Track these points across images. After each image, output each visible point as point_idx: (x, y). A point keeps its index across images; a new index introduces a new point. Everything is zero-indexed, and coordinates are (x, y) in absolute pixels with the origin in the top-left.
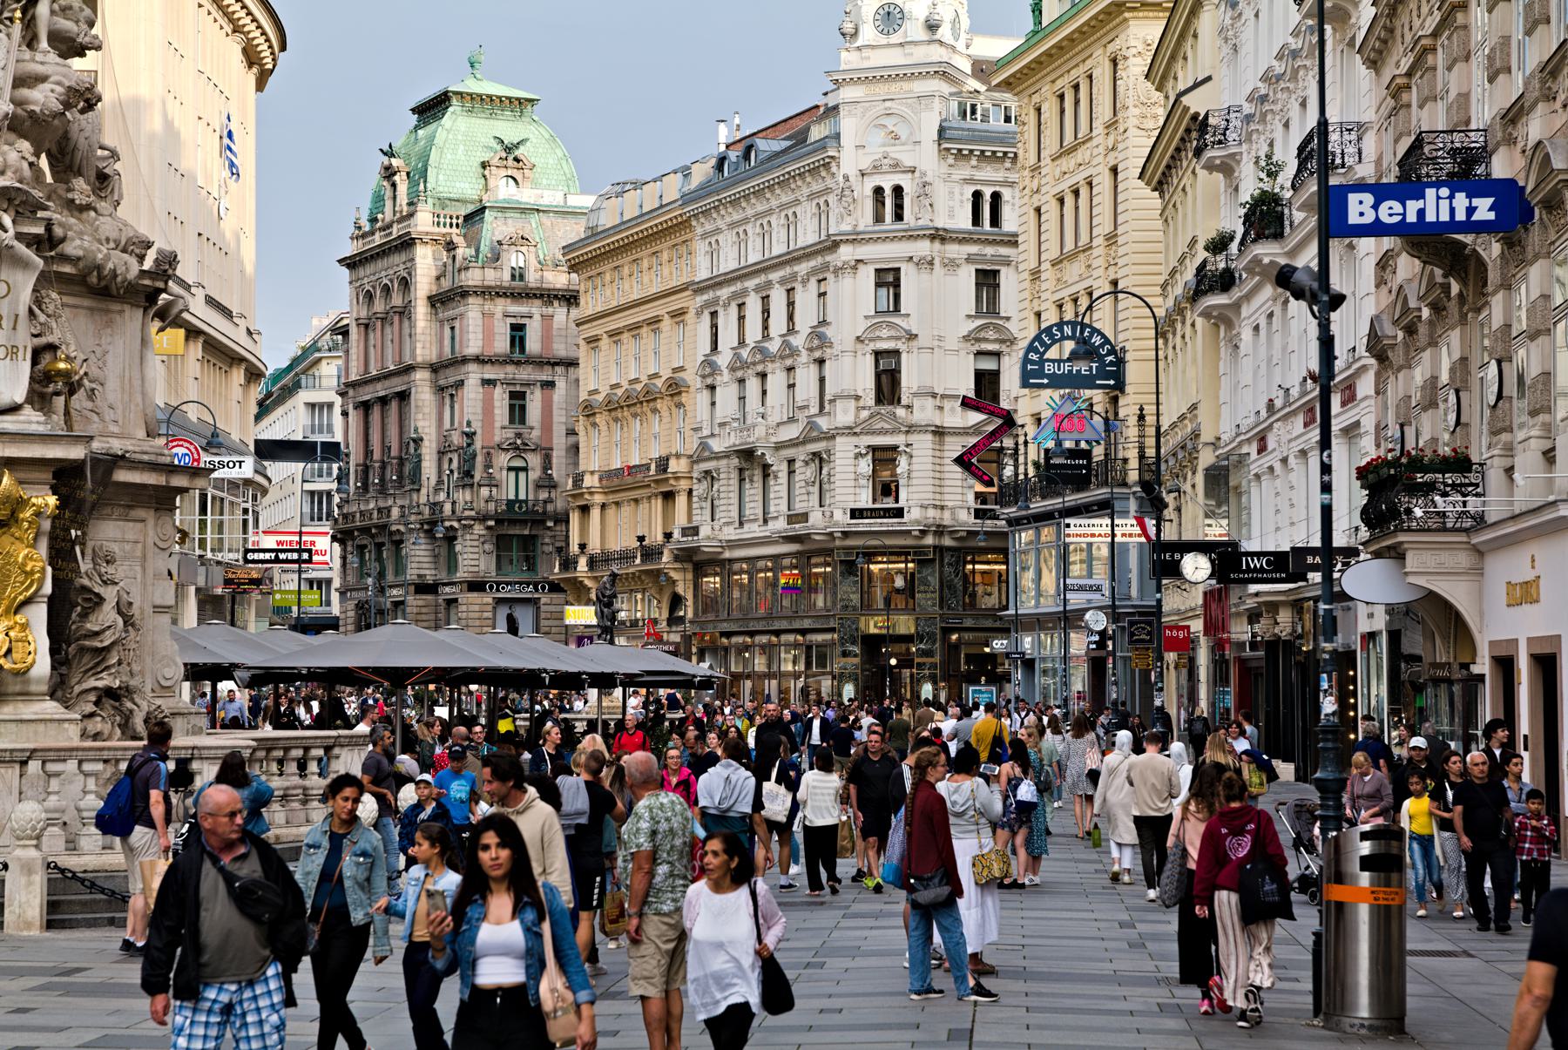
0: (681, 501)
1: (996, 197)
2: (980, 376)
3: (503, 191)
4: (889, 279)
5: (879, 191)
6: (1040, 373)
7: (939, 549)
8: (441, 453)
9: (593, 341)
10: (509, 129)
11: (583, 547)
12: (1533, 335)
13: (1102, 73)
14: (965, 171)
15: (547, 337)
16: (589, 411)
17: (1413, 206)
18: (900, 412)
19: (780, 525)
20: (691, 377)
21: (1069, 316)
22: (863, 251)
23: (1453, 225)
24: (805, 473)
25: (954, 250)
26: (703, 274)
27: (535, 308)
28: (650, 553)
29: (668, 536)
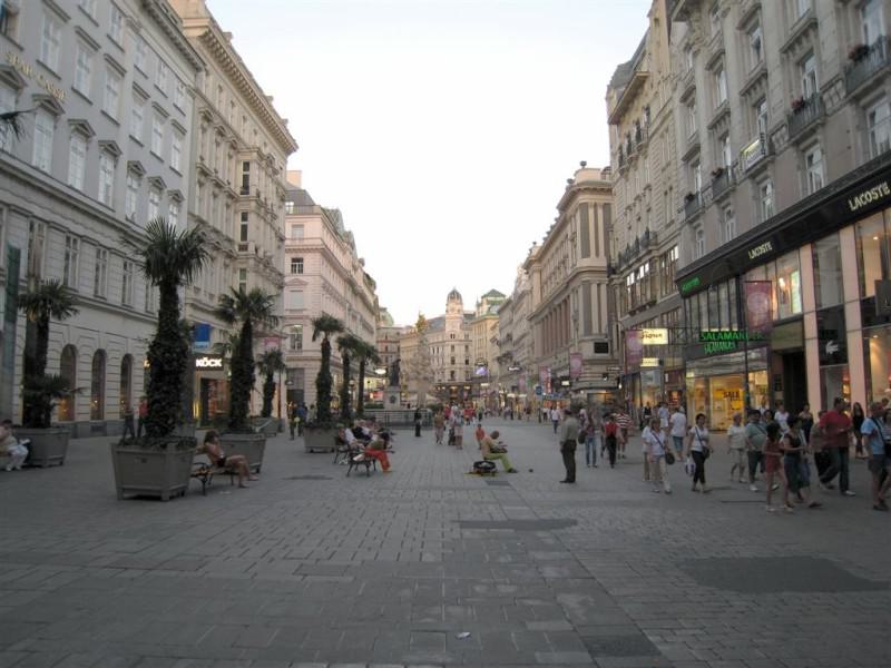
4: (453, 347)
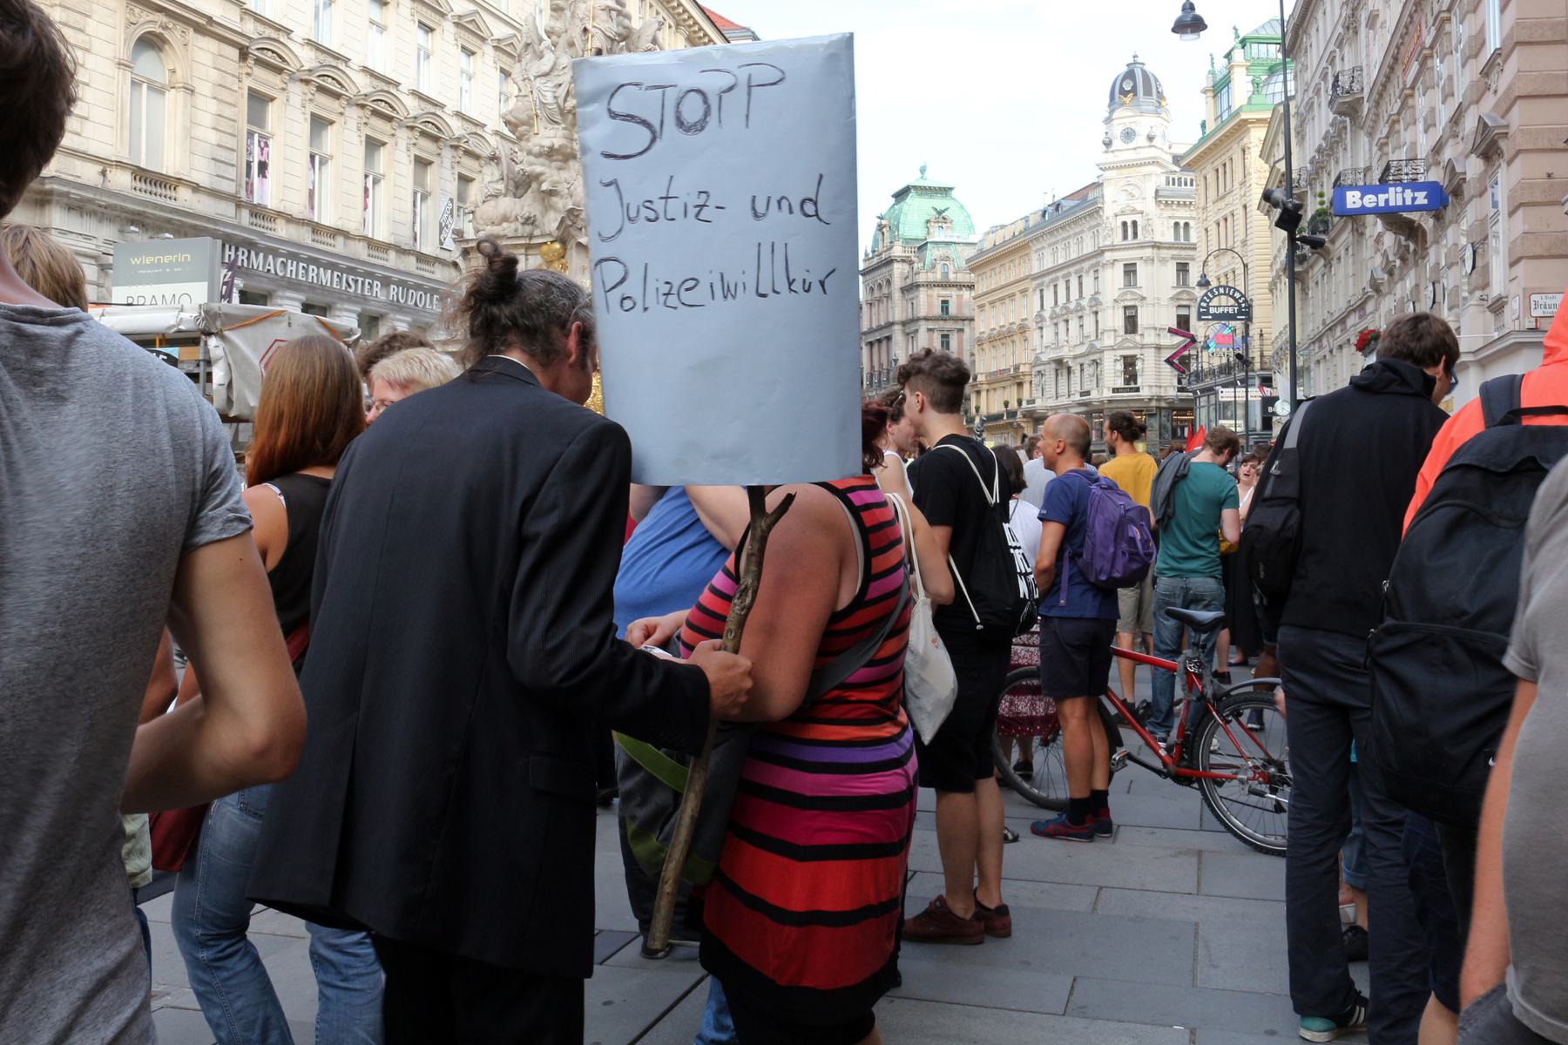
0: (1026, 386)
1: (1186, 224)
2: (1179, 317)
3: (938, 235)
4: (1130, 270)
5: (1125, 224)
6: (1207, 313)
7: (1159, 408)
9: (981, 307)
10: (940, 203)
11: (977, 409)
12: (1450, 266)
13: (1237, 157)
14: (1170, 213)
15: (960, 305)
16: (980, 342)
17: (1382, 197)
18: (1137, 338)
19: (1077, 397)
20: (1032, 324)
21: (1223, 283)
22: (1116, 255)
23: (1405, 208)
24: (1089, 370)
25: (1165, 253)
26: (1036, 270)
27: (953, 292)
28: (1013, 414)
29: (1020, 402)
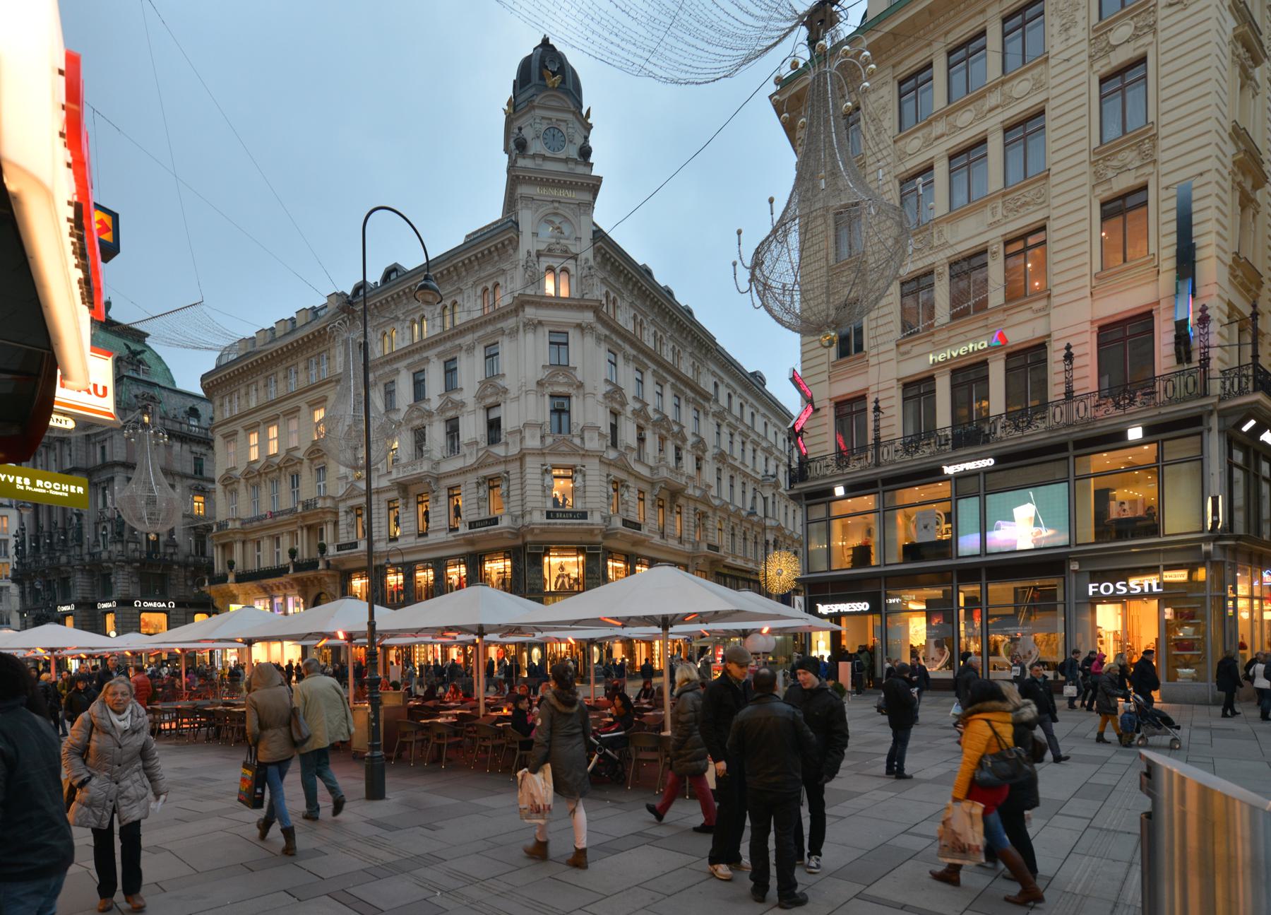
8: (97, 524)
